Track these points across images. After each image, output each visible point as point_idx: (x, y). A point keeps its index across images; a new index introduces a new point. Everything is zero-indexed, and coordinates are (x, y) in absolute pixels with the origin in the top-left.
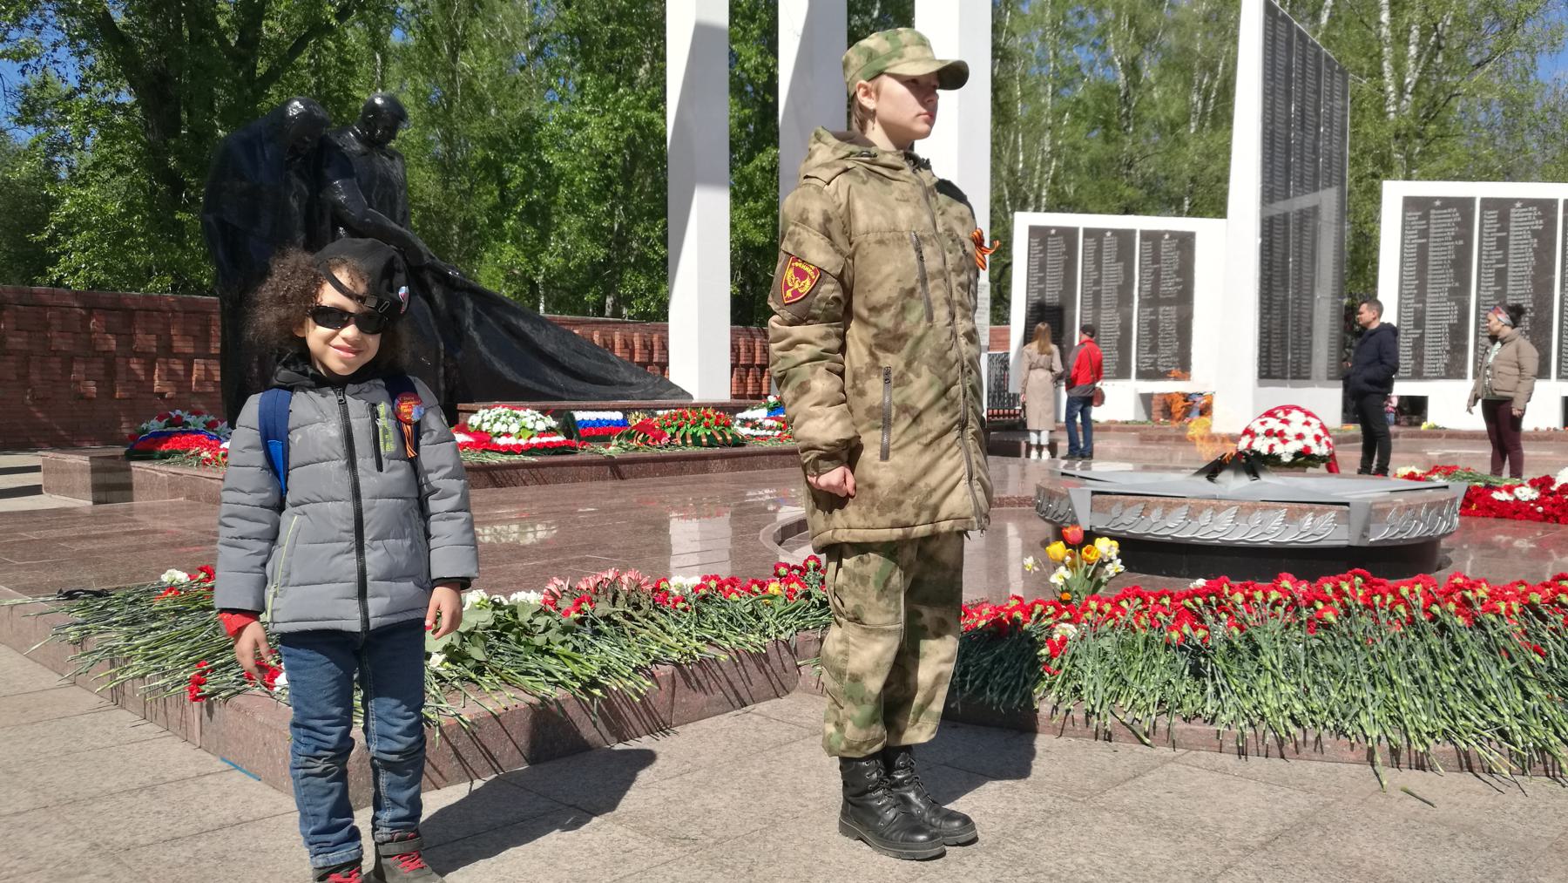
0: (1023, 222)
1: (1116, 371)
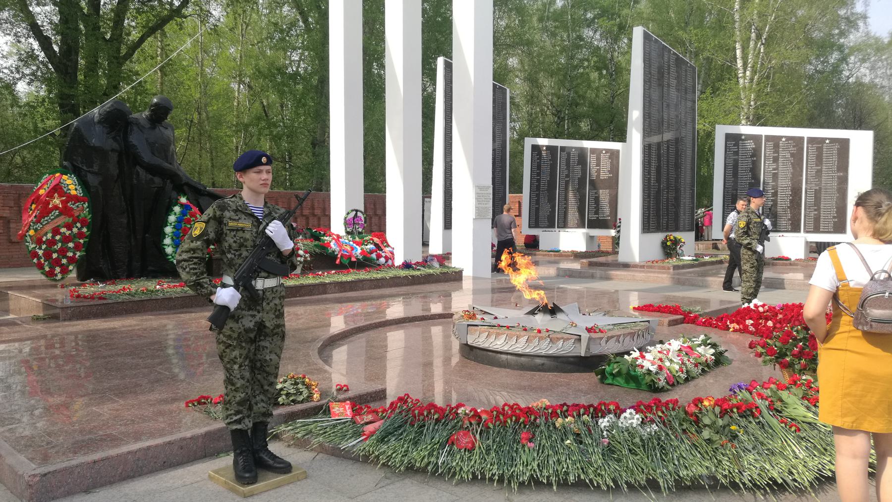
0: (529, 142)
1: (577, 224)
